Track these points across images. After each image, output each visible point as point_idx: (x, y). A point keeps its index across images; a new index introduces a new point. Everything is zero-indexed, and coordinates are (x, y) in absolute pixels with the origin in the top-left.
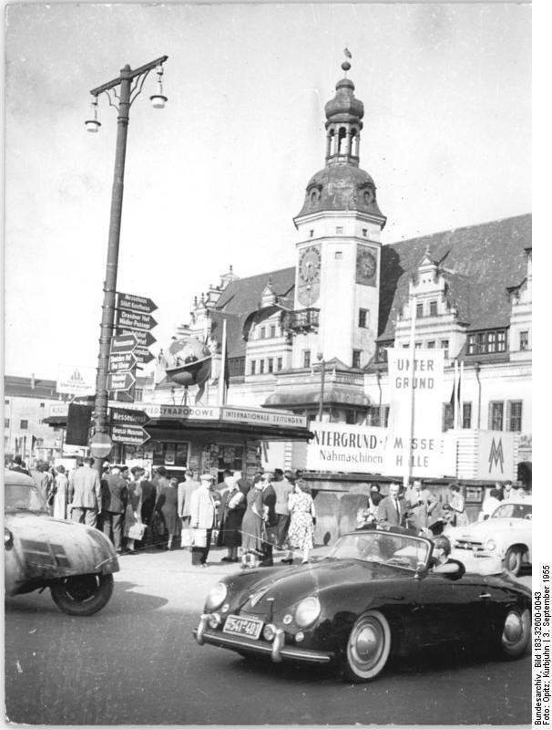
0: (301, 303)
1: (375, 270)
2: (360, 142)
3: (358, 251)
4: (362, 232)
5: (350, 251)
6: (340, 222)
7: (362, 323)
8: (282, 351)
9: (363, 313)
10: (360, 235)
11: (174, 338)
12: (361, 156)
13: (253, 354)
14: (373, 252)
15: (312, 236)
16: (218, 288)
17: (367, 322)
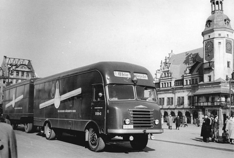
0: (206, 60)
1: (231, 48)
2: (223, 5)
3: (226, 41)
4: (227, 36)
5: (223, 42)
6: (219, 32)
7: (228, 66)
8: (197, 77)
9: (228, 63)
10: (226, 36)
11: (155, 74)
12: (223, 9)
13: (186, 78)
14: (230, 42)
15: (209, 37)
16: (168, 58)
17: (230, 66)
